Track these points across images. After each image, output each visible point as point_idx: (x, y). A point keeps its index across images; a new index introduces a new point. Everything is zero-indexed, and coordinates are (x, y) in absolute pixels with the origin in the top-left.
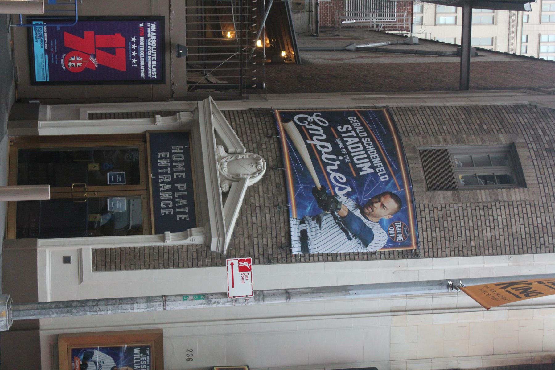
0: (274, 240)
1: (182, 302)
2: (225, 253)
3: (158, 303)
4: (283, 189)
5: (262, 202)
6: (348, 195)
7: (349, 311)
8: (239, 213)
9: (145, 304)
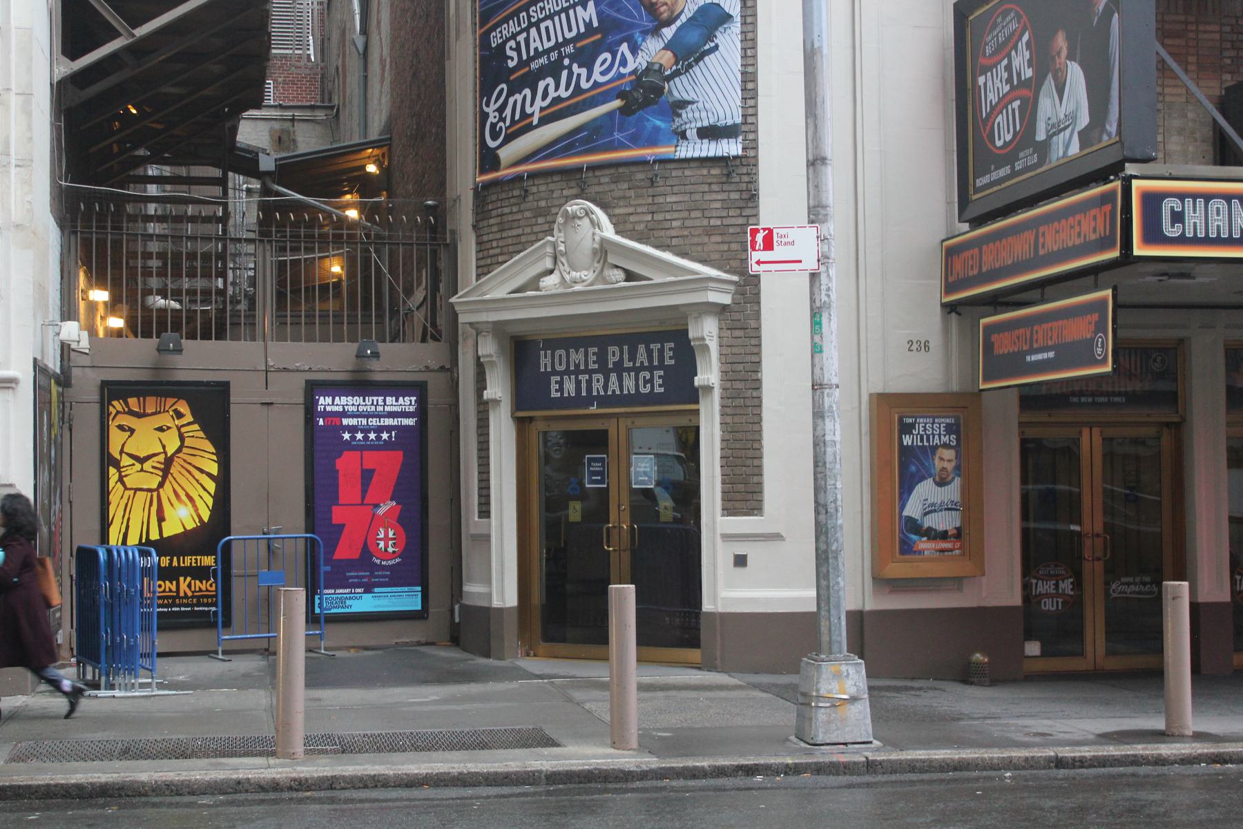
0: (715, 187)
1: (824, 355)
2: (735, 278)
3: (826, 398)
4: (621, 170)
5: (644, 209)
6: (634, 50)
7: (849, 51)
8: (664, 251)
9: (827, 420)
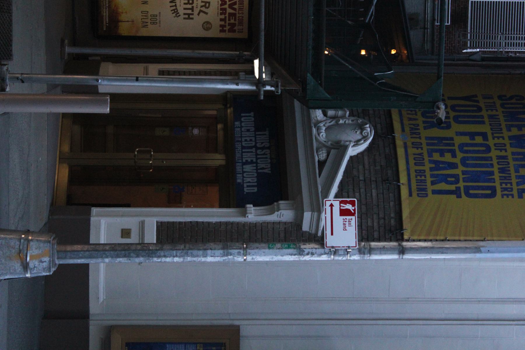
0: (382, 221)
1: (267, 251)
3: (237, 251)
4: (393, 161)
8: (339, 187)
9: (221, 251)
